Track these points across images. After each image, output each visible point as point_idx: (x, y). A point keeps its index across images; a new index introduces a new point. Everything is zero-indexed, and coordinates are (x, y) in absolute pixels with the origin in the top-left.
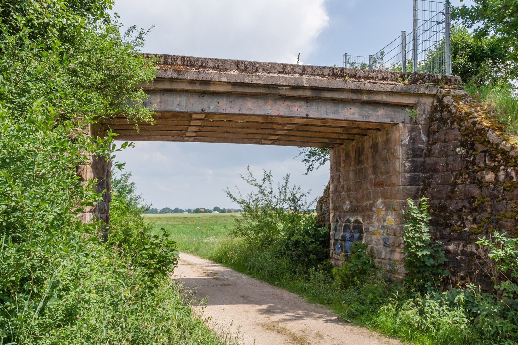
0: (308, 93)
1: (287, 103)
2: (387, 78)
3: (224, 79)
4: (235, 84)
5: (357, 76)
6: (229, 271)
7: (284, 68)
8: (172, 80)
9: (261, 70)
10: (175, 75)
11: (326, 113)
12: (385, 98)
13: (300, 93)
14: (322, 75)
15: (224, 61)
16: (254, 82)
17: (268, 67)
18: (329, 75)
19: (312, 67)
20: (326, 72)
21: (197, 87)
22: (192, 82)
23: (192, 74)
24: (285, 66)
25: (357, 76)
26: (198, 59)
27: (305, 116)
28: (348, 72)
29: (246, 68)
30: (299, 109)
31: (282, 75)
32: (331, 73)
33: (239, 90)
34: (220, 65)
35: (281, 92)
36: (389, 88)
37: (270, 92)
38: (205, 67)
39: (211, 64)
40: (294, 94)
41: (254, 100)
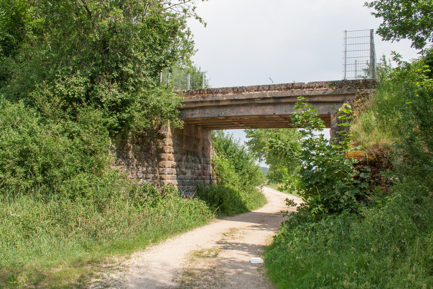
0: (272, 101)
1: (262, 107)
2: (322, 86)
3: (225, 99)
4: (231, 100)
5: (302, 87)
6: (256, 208)
7: (258, 88)
8: (202, 102)
9: (245, 91)
10: (202, 99)
11: (286, 111)
12: (321, 99)
13: (267, 101)
14: (280, 89)
15: (227, 88)
16: (240, 98)
17: (248, 89)
18: (284, 89)
19: (274, 85)
20: (283, 87)
21: (214, 104)
22: (211, 101)
23: (210, 98)
24: (259, 86)
25: (302, 87)
26: (214, 89)
27: (273, 114)
28: (296, 85)
29: (238, 90)
30: (269, 110)
31: (257, 92)
32: (286, 88)
33: (234, 103)
34: (225, 91)
35: (257, 102)
36: (321, 93)
37: (250, 102)
38: (217, 93)
39: (220, 91)
40: (264, 102)
41: (244, 107)
